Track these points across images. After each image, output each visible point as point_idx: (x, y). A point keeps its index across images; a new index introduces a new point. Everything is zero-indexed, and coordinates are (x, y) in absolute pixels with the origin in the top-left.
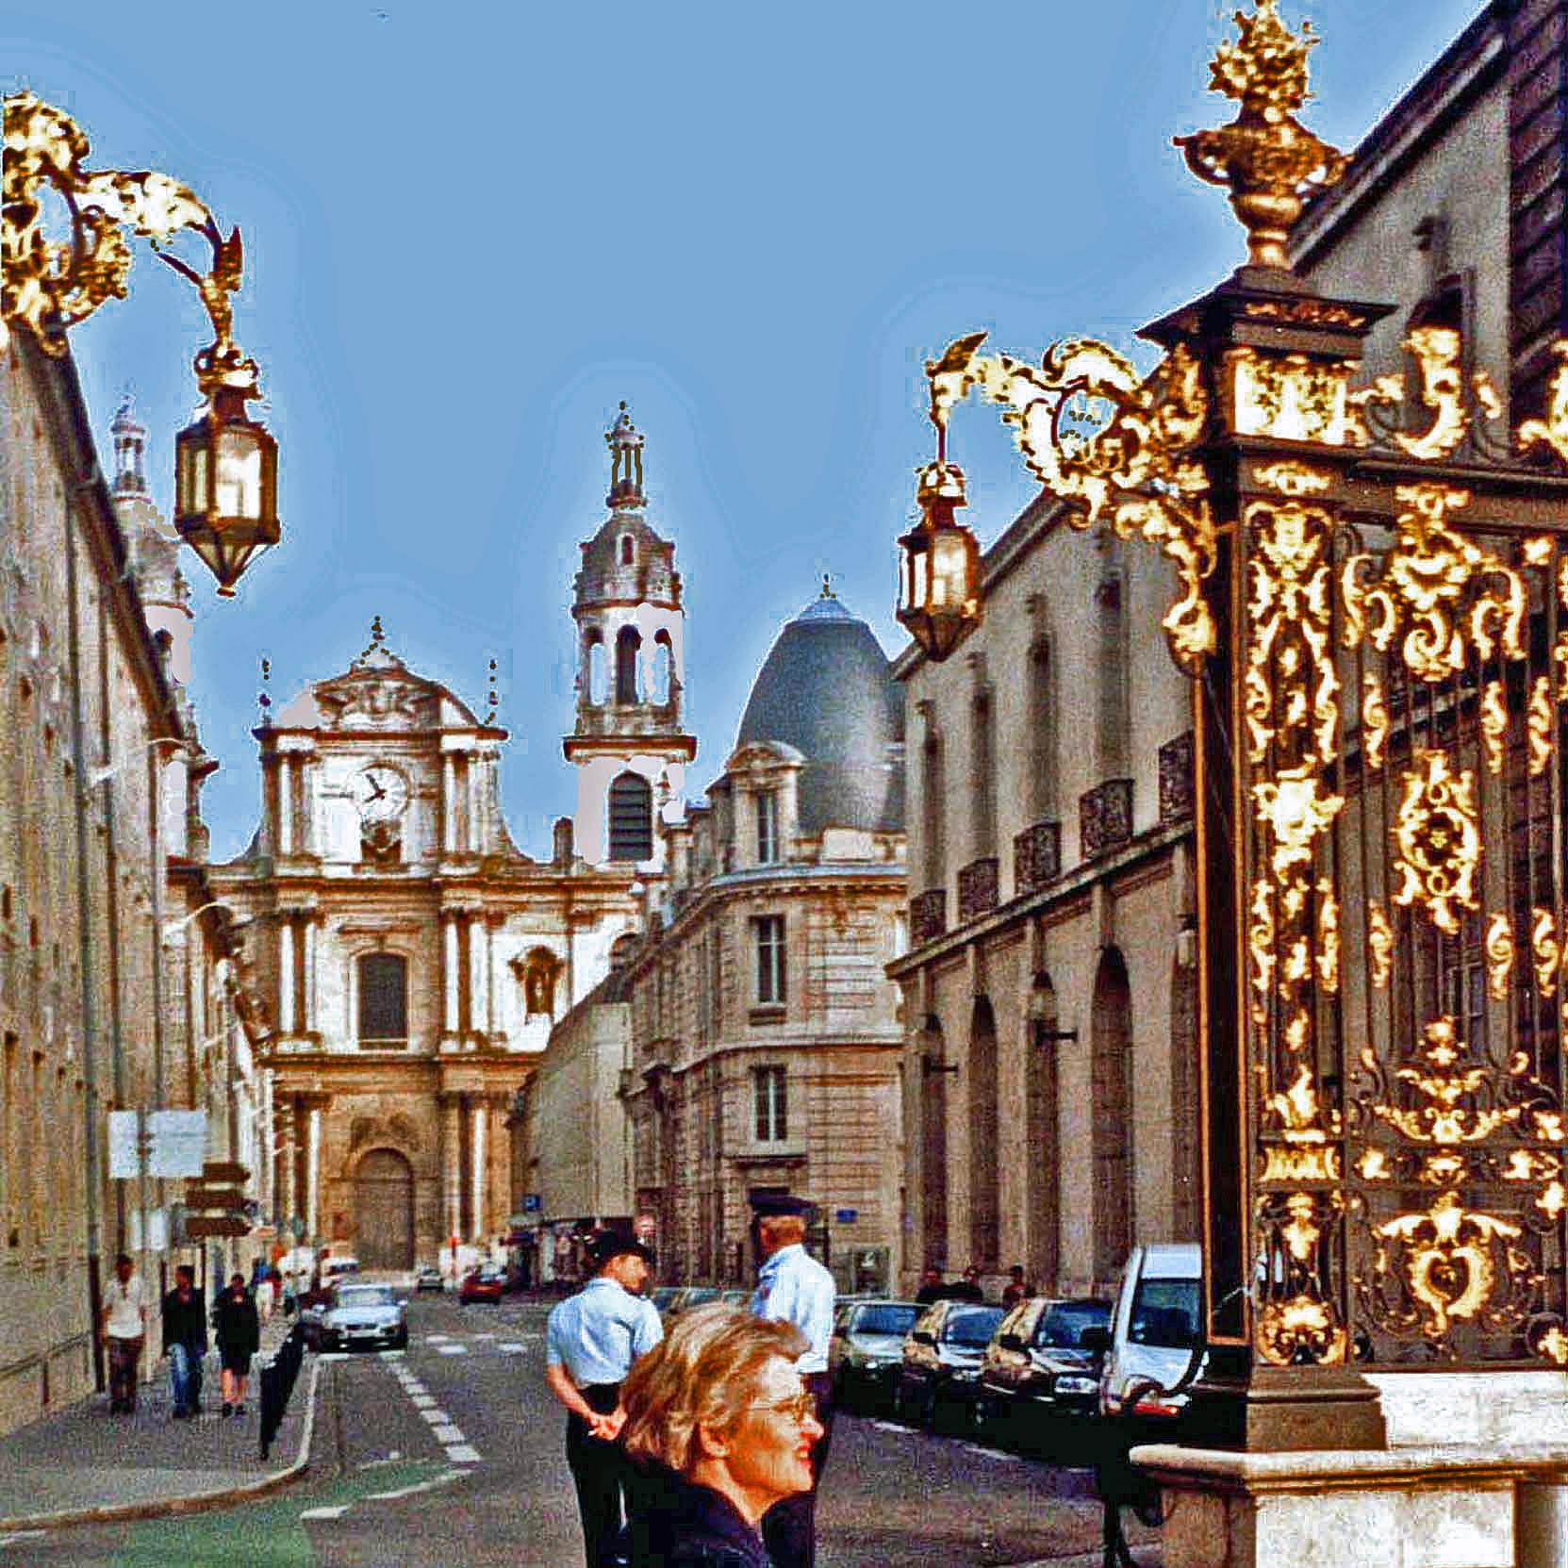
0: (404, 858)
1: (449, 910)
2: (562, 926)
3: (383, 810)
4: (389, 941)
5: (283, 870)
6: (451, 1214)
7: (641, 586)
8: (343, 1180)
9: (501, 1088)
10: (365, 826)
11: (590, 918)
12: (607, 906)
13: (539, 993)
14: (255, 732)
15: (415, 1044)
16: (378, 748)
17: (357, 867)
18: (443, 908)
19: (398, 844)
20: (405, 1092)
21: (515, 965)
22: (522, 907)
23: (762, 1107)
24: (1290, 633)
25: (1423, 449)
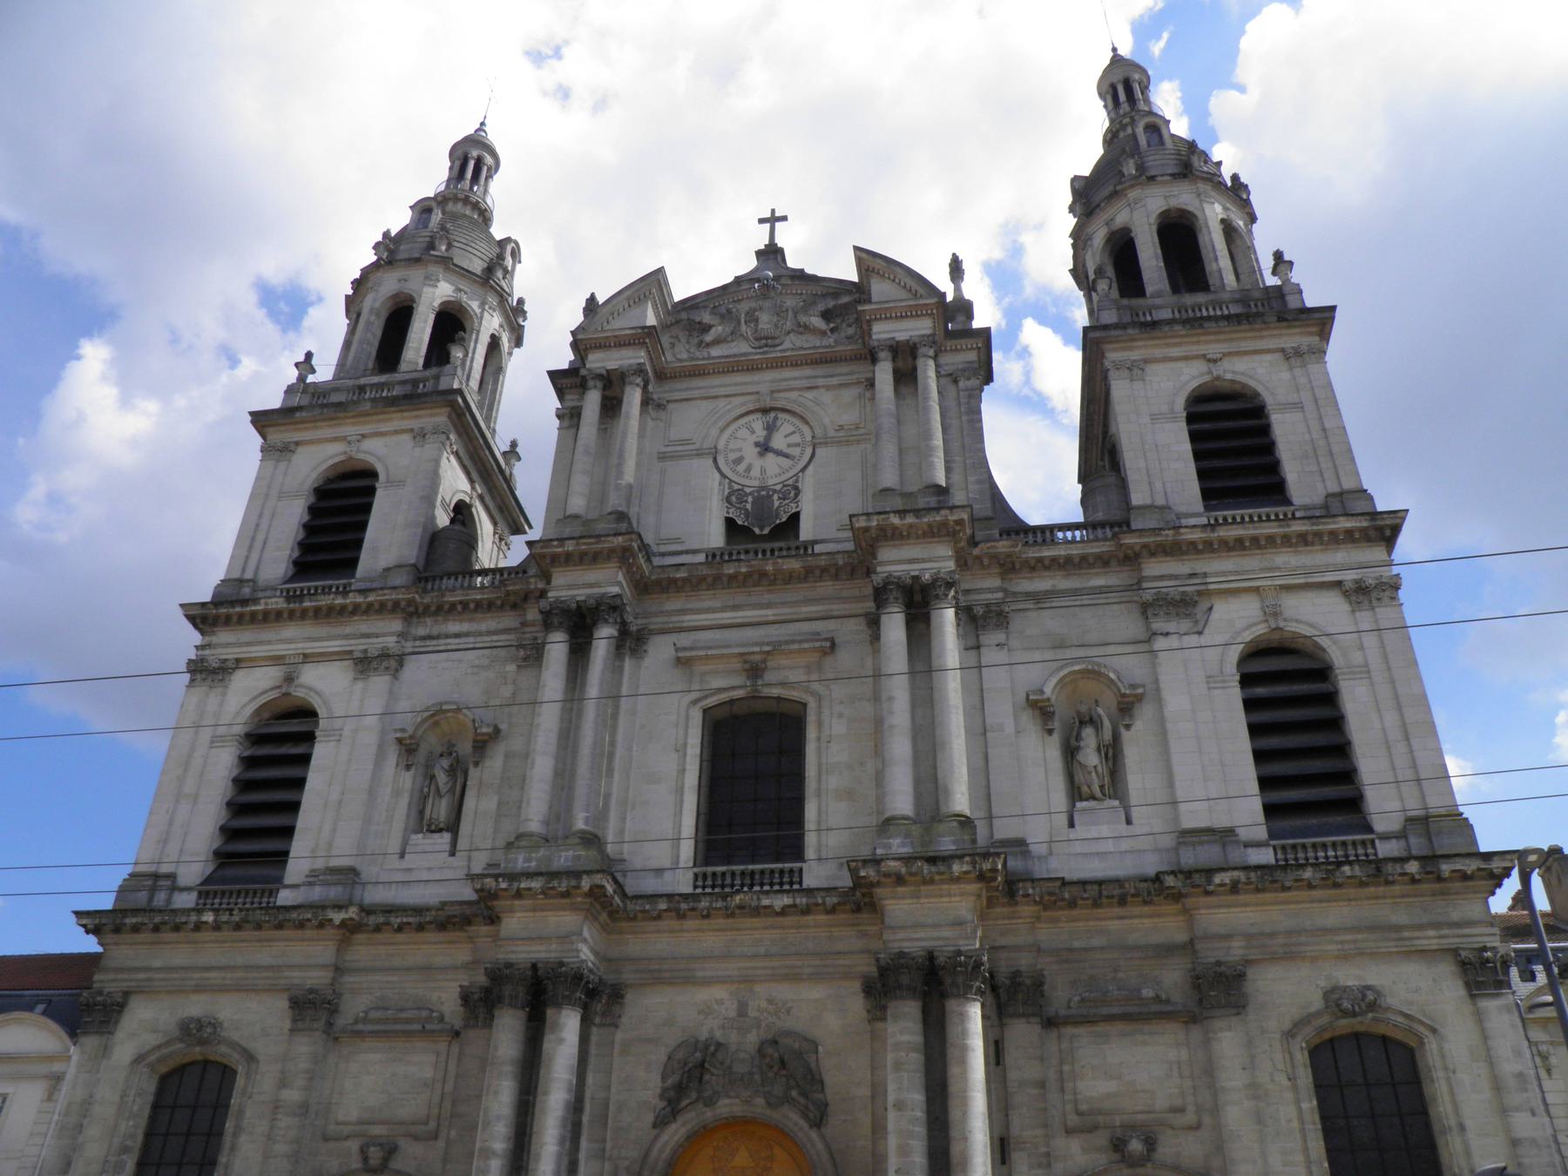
0: (806, 531)
3: (772, 471)
4: (769, 677)
9: (1024, 961)
10: (734, 496)
11: (1186, 605)
13: (1090, 757)
14: (554, 375)
15: (815, 874)
16: (764, 381)
17: (712, 555)
18: (877, 579)
19: (795, 518)
20: (794, 977)
21: (1041, 710)
22: (1039, 599)
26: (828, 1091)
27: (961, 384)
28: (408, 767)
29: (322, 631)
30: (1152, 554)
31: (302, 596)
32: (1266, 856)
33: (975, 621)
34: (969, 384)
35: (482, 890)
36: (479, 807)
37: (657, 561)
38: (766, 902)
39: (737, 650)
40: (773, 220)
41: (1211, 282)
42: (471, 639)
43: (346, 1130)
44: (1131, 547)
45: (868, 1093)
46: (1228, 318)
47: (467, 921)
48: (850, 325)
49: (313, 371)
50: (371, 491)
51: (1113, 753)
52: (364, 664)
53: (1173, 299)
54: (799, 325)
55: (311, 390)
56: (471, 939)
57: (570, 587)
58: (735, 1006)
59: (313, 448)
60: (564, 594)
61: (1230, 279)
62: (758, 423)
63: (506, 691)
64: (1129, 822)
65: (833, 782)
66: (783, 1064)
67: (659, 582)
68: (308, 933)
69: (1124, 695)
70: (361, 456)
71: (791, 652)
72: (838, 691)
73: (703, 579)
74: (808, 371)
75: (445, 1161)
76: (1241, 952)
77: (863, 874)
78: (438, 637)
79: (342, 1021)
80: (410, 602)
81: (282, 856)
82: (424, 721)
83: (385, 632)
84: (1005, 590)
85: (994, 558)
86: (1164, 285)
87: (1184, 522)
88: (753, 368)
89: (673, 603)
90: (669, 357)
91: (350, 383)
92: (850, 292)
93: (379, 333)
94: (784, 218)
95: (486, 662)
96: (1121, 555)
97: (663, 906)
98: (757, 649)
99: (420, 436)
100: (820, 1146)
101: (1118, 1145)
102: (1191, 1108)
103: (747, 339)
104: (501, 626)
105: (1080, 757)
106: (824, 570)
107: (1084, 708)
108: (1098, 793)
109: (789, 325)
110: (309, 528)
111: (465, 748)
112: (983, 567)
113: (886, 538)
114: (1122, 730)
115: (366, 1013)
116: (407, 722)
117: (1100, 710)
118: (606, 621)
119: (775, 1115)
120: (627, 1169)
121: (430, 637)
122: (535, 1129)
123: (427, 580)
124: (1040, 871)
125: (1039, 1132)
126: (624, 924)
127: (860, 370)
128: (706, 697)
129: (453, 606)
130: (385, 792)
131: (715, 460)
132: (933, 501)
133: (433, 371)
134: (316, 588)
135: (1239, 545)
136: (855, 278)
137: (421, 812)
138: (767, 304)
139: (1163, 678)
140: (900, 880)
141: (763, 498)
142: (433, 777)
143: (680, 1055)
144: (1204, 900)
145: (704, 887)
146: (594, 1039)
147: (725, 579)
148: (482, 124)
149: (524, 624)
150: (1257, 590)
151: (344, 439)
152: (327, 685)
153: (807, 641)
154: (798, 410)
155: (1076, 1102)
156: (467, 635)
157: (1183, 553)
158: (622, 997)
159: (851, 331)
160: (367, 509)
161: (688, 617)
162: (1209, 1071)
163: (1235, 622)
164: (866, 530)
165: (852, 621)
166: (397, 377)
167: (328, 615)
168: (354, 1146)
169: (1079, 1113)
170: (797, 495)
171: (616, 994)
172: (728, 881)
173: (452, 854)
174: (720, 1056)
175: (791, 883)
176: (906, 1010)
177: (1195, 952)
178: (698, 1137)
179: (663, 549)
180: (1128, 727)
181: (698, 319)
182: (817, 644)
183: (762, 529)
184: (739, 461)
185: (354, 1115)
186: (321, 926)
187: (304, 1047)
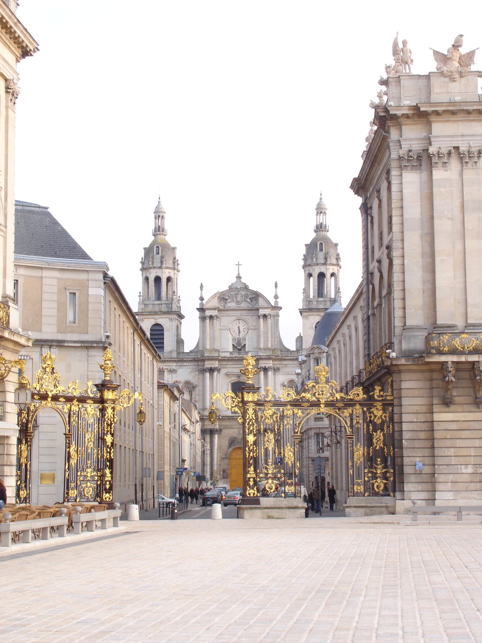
0: (247, 350)
4: (241, 378)
5: (207, 354)
7: (326, 259)
8: (226, 458)
14: (198, 309)
16: (238, 313)
18: (259, 367)
23: (318, 442)
24: (251, 420)
25: (268, 399)
40: (239, 265)
62: (237, 322)
63: (197, 377)
74: (247, 312)
83: (173, 366)
88: (236, 310)
89: (225, 363)
99: (171, 319)
160: (163, 334)
171: (221, 430)
179: (222, 351)
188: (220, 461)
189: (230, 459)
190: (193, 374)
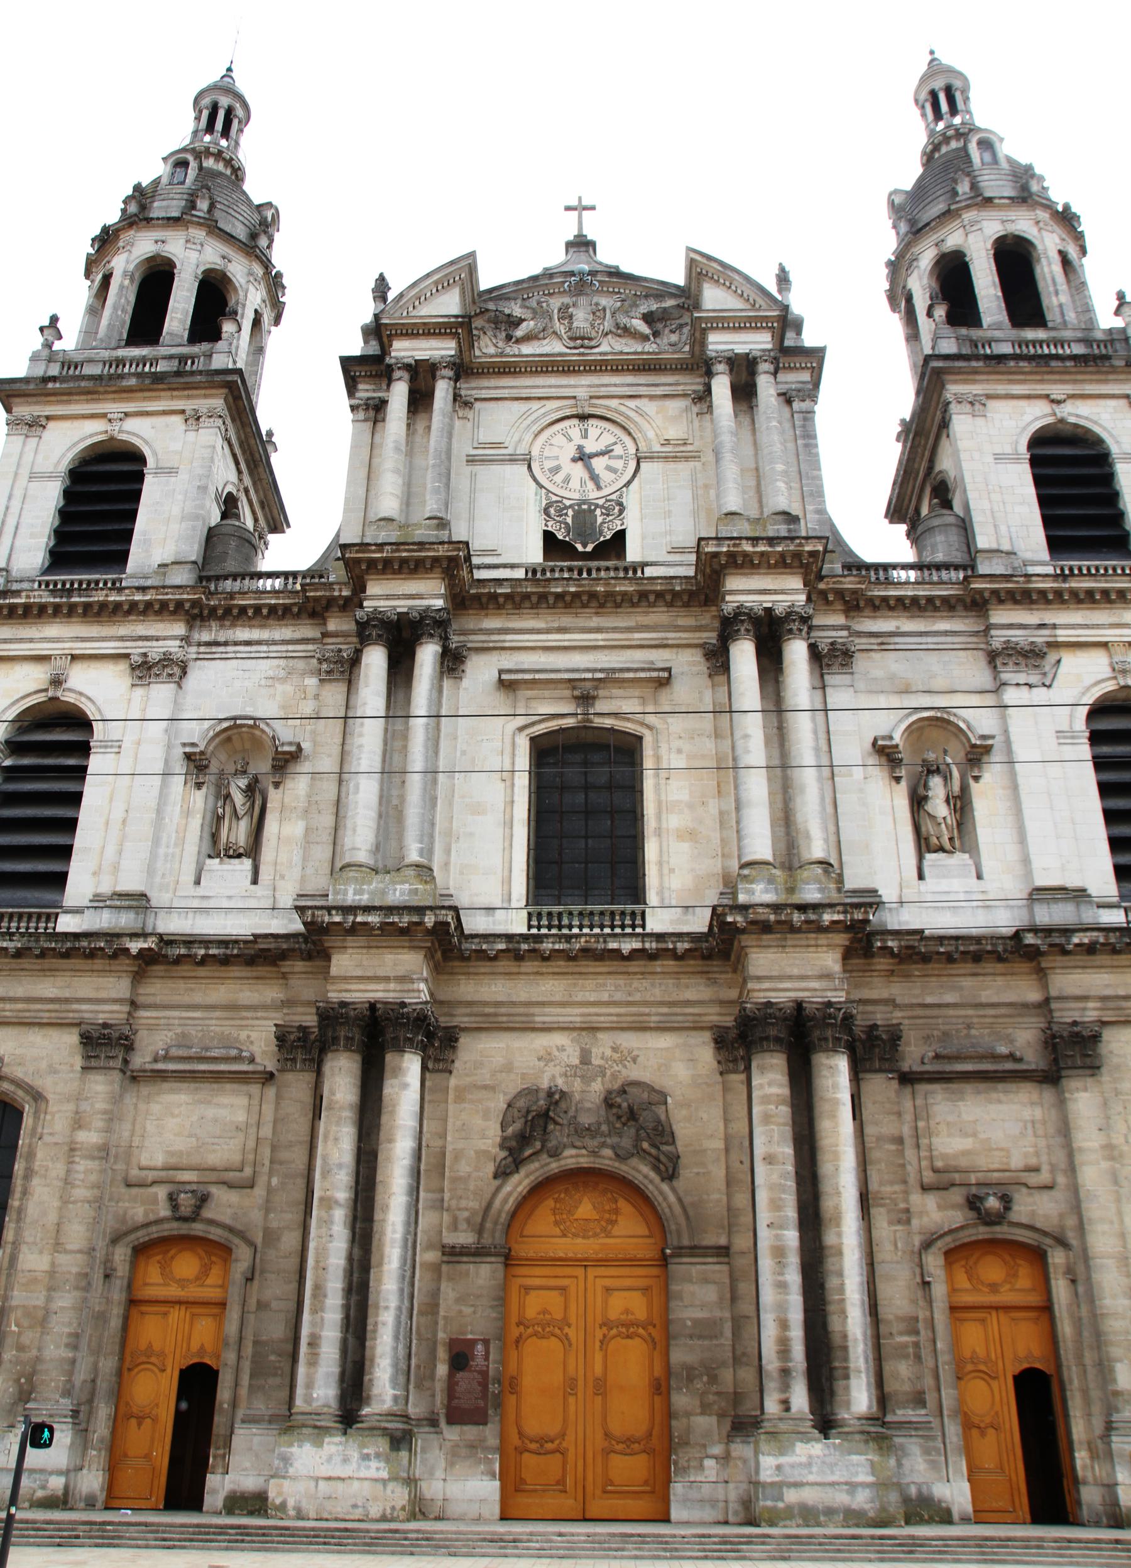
0: (634, 552)
1: (740, 614)
2: (981, 676)
4: (601, 706)
6: (784, 1351)
8: (477, 1253)
9: (880, 1016)
12: (1063, 635)
13: (939, 807)
14: (347, 363)
16: (581, 386)
19: (620, 536)
26: (679, 1143)
27: (796, 405)
28: (199, 785)
29: (94, 630)
30: (1001, 601)
31: (70, 592)
32: (1116, 917)
33: (828, 660)
34: (804, 406)
35: (312, 923)
36: (283, 831)
37: (480, 574)
38: (613, 945)
39: (566, 676)
41: (1049, 317)
42: (264, 648)
43: (151, 1176)
44: (980, 592)
45: (720, 1145)
46: (1074, 358)
47: (283, 955)
48: (672, 332)
49: (60, 337)
50: (140, 477)
51: (961, 803)
52: (145, 670)
53: (1014, 333)
54: (618, 326)
55: (60, 357)
56: (284, 976)
57: (388, 597)
58: (577, 1053)
59: (66, 424)
60: (382, 604)
61: (1071, 316)
62: (573, 428)
64: (979, 877)
65: (673, 821)
66: (632, 1115)
67: (478, 597)
68: (98, 963)
69: (974, 746)
70: (123, 437)
71: (624, 680)
72: (676, 724)
73: (527, 596)
74: (630, 379)
75: (268, 1207)
76: (1095, 1013)
77: (730, 919)
78: (226, 644)
79: (140, 1060)
80: (195, 603)
81: (59, 880)
82: (217, 735)
83: (165, 637)
84: (847, 628)
85: (840, 594)
86: (1003, 317)
87: (1031, 570)
89: (492, 622)
90: (477, 353)
91: (106, 354)
92: (673, 296)
93: (132, 298)
94: (593, 208)
95: (282, 674)
96: (968, 600)
97: (502, 946)
98: (589, 676)
100: (672, 1198)
101: (974, 1203)
102: (1045, 1168)
103: (560, 338)
104: (298, 635)
105: (929, 807)
106: (659, 595)
107: (931, 756)
108: (947, 846)
109: (608, 325)
110: (64, 514)
111: (262, 766)
112: (828, 602)
113: (737, 566)
114: (971, 782)
115: (167, 1051)
116: (196, 733)
117: (949, 760)
118: (432, 636)
119: (623, 1169)
120: (468, 1221)
121: (217, 644)
122: (379, 1178)
123: (209, 579)
124: (893, 924)
125: (897, 1188)
126: (456, 963)
127: (691, 383)
128: (533, 724)
129: (243, 610)
130: (174, 811)
131: (529, 467)
132: (782, 530)
133: (205, 346)
134: (81, 583)
135: (1088, 599)
136: (681, 282)
137: (215, 837)
138: (582, 300)
139: (1012, 730)
140: (766, 928)
141: (584, 515)
142: (228, 796)
143: (521, 1103)
144: (1060, 960)
145: (539, 927)
146: (428, 1084)
147: (551, 600)
148: (229, 70)
149: (325, 635)
150: (1105, 645)
151: (104, 415)
152: (100, 689)
153: (643, 670)
154: (620, 419)
155: (931, 1157)
156: (259, 643)
157: (1032, 602)
158: (457, 1040)
159: (674, 338)
160: (136, 496)
161: (509, 637)
162: (1065, 1130)
163: (1085, 677)
164: (715, 555)
165: (689, 651)
166: (162, 351)
167: (98, 614)
168: (162, 1192)
169: (935, 1171)
170: (621, 512)
172: (565, 921)
173: (255, 881)
174: (563, 1105)
175: (633, 927)
176: (775, 1061)
177: (1051, 1011)
178: (539, 1189)
180: (977, 779)
181: (507, 311)
182: (655, 674)
183: (585, 546)
184: (556, 470)
185: (159, 1160)
186: (115, 956)
187: (101, 1086)
188: (435, 1269)
189: (508, 1259)
190: (287, 689)
